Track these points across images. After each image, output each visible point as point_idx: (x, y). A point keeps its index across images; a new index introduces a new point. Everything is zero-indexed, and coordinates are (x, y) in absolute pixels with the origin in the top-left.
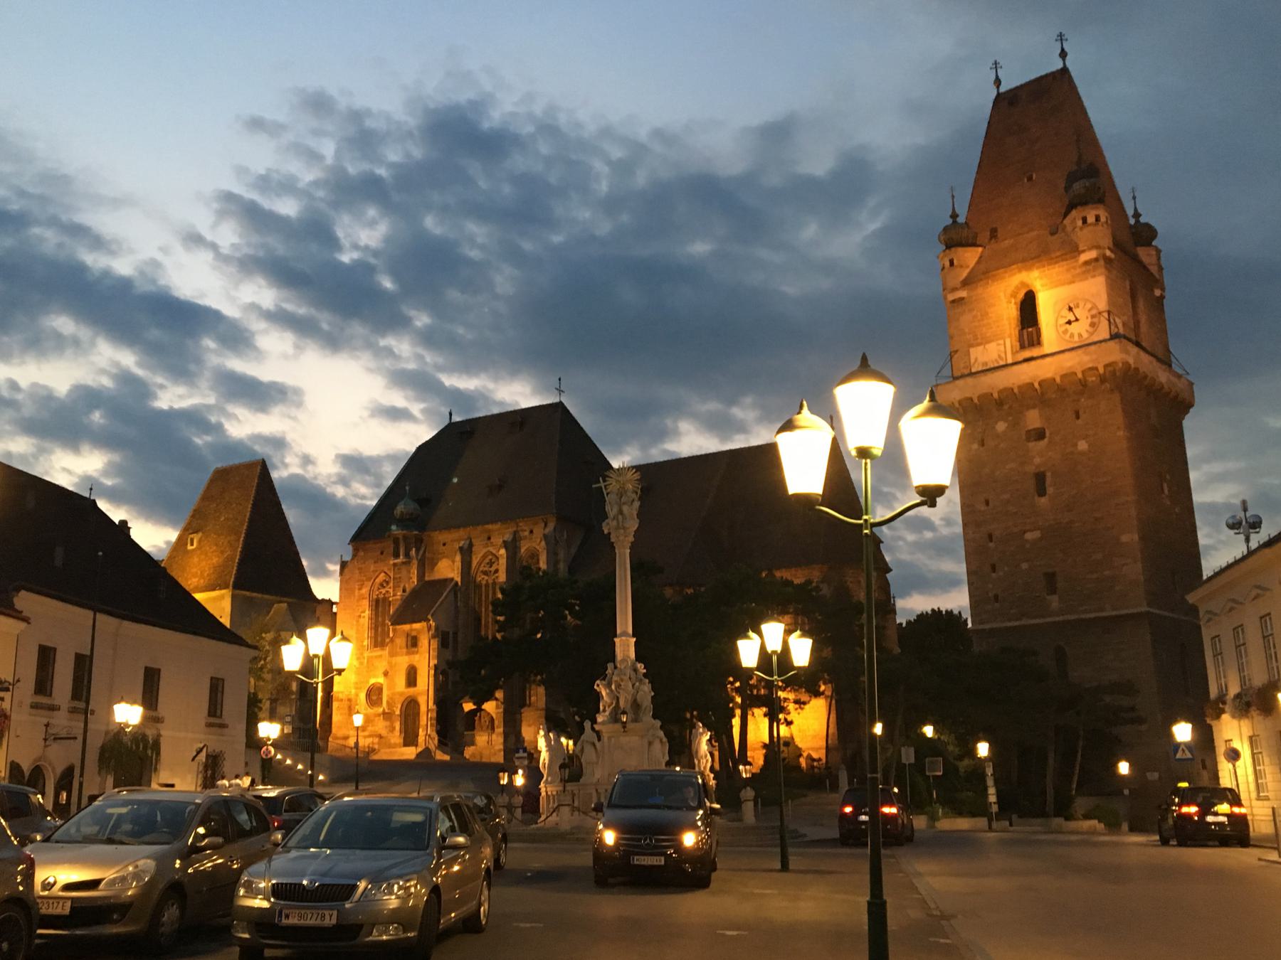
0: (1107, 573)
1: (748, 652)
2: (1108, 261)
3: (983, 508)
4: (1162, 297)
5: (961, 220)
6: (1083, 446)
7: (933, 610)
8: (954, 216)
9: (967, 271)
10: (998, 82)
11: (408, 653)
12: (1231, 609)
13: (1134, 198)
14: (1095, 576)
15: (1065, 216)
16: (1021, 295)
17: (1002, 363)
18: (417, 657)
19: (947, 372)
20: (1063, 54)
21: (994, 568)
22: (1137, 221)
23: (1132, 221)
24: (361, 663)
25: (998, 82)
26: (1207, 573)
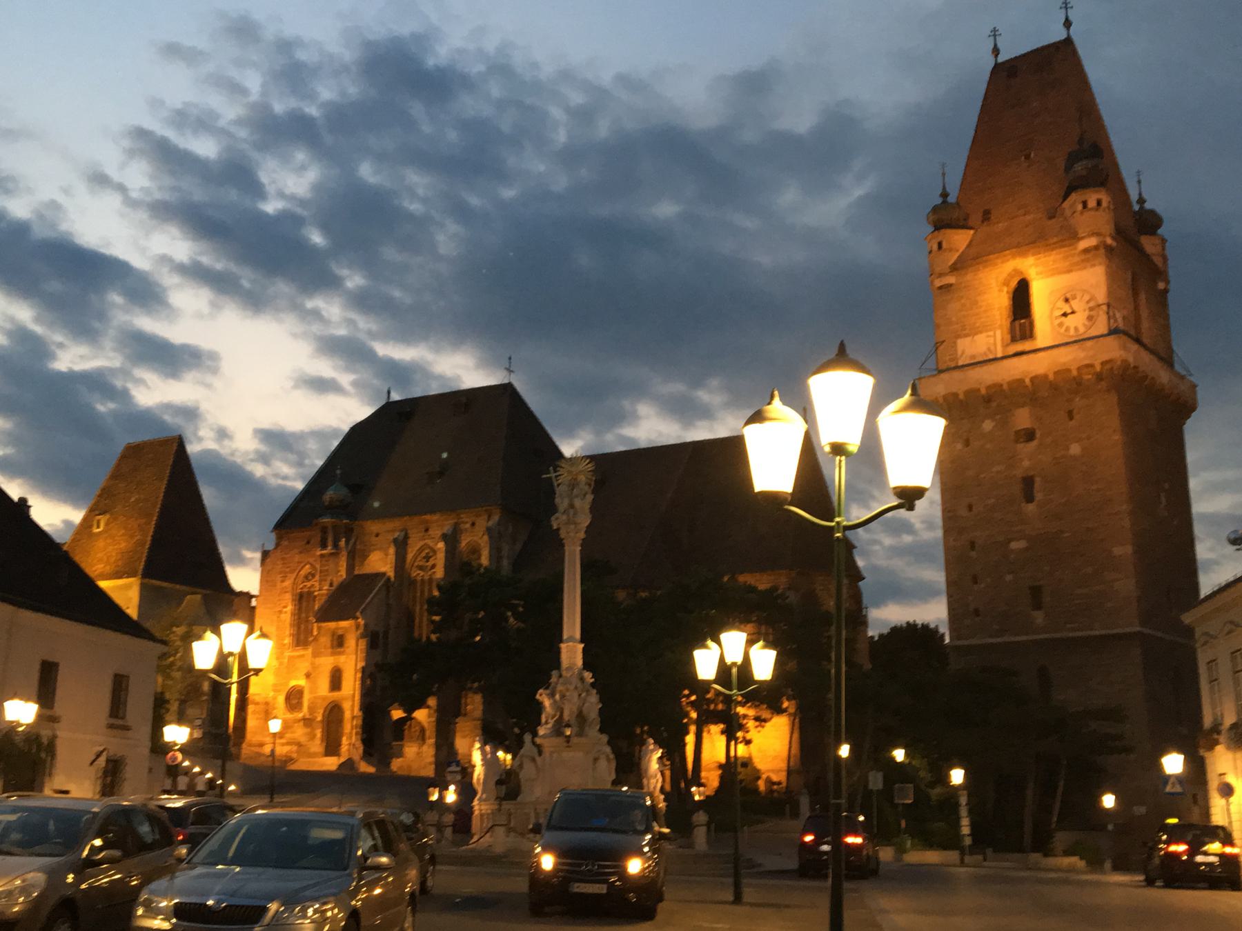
1: (705, 663)
2: (1109, 250)
4: (1166, 291)
5: (952, 199)
6: (1075, 449)
7: (908, 623)
8: (945, 195)
9: (957, 254)
10: (996, 51)
11: (333, 654)
12: (1230, 632)
13: (1139, 182)
15: (1064, 200)
16: (1014, 284)
17: (991, 357)
18: (342, 658)
19: (931, 364)
20: (1068, 24)
21: (975, 580)
22: (1142, 208)
23: (1136, 207)
24: (281, 664)
25: (996, 51)
26: (1204, 591)
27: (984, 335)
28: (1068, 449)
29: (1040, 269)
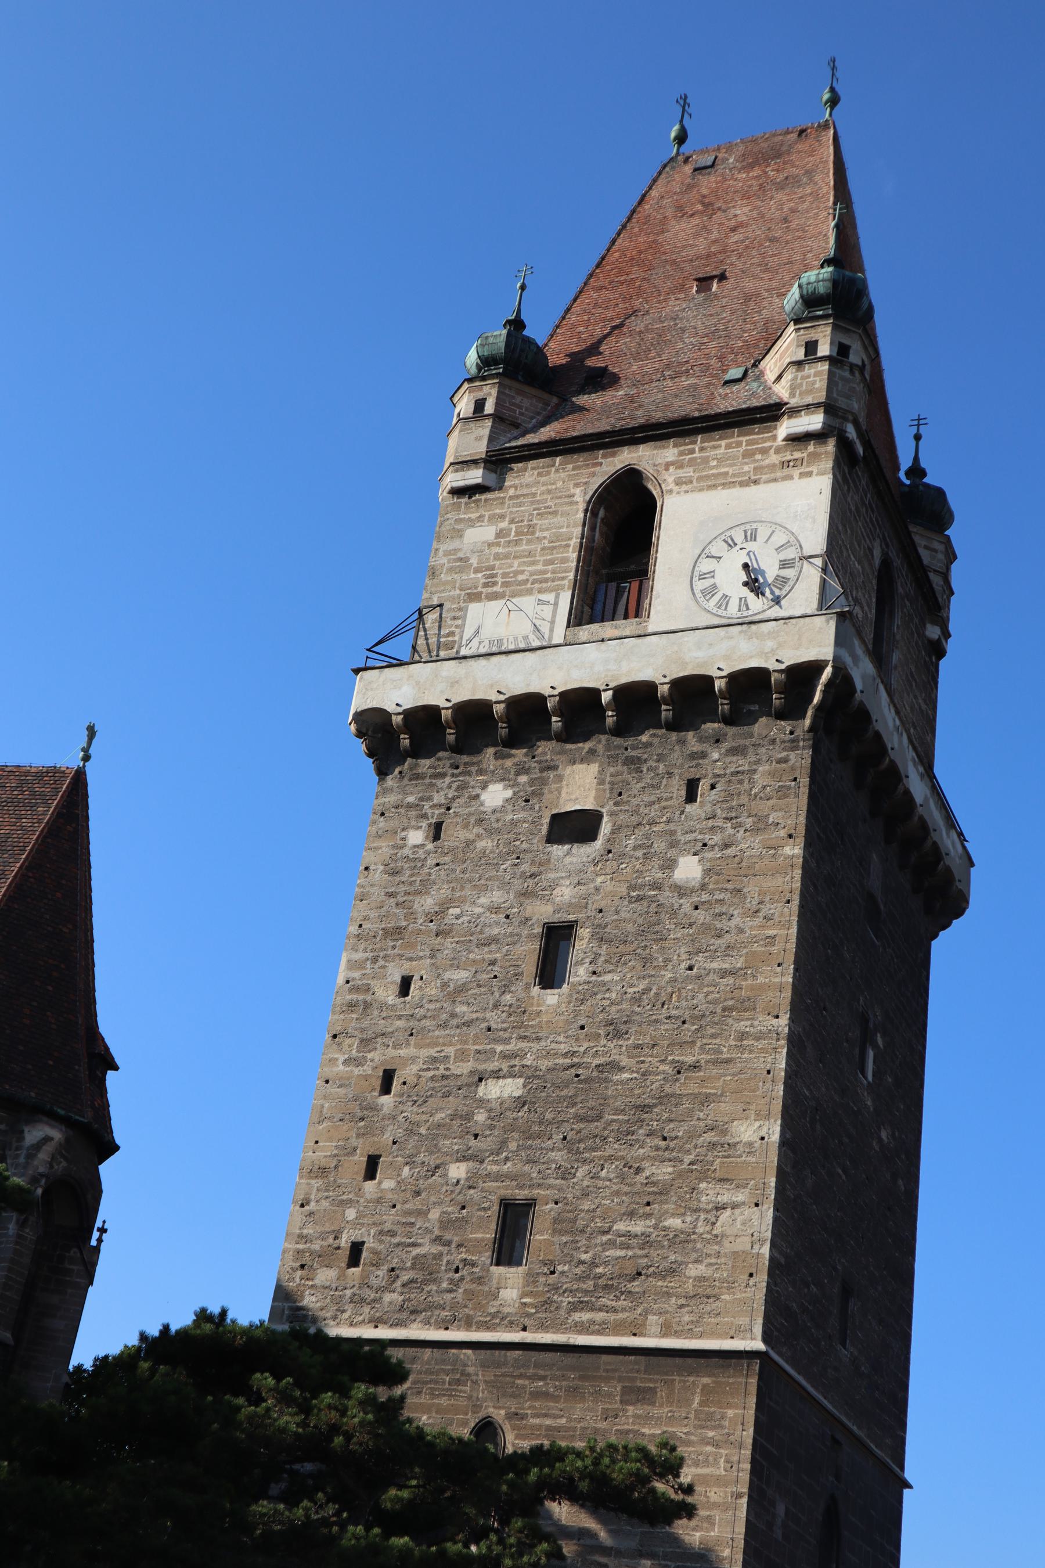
0: (675, 1222)
2: (844, 447)
4: (938, 651)
13: (918, 437)
14: (638, 1227)
28: (670, 865)
29: (688, 472)
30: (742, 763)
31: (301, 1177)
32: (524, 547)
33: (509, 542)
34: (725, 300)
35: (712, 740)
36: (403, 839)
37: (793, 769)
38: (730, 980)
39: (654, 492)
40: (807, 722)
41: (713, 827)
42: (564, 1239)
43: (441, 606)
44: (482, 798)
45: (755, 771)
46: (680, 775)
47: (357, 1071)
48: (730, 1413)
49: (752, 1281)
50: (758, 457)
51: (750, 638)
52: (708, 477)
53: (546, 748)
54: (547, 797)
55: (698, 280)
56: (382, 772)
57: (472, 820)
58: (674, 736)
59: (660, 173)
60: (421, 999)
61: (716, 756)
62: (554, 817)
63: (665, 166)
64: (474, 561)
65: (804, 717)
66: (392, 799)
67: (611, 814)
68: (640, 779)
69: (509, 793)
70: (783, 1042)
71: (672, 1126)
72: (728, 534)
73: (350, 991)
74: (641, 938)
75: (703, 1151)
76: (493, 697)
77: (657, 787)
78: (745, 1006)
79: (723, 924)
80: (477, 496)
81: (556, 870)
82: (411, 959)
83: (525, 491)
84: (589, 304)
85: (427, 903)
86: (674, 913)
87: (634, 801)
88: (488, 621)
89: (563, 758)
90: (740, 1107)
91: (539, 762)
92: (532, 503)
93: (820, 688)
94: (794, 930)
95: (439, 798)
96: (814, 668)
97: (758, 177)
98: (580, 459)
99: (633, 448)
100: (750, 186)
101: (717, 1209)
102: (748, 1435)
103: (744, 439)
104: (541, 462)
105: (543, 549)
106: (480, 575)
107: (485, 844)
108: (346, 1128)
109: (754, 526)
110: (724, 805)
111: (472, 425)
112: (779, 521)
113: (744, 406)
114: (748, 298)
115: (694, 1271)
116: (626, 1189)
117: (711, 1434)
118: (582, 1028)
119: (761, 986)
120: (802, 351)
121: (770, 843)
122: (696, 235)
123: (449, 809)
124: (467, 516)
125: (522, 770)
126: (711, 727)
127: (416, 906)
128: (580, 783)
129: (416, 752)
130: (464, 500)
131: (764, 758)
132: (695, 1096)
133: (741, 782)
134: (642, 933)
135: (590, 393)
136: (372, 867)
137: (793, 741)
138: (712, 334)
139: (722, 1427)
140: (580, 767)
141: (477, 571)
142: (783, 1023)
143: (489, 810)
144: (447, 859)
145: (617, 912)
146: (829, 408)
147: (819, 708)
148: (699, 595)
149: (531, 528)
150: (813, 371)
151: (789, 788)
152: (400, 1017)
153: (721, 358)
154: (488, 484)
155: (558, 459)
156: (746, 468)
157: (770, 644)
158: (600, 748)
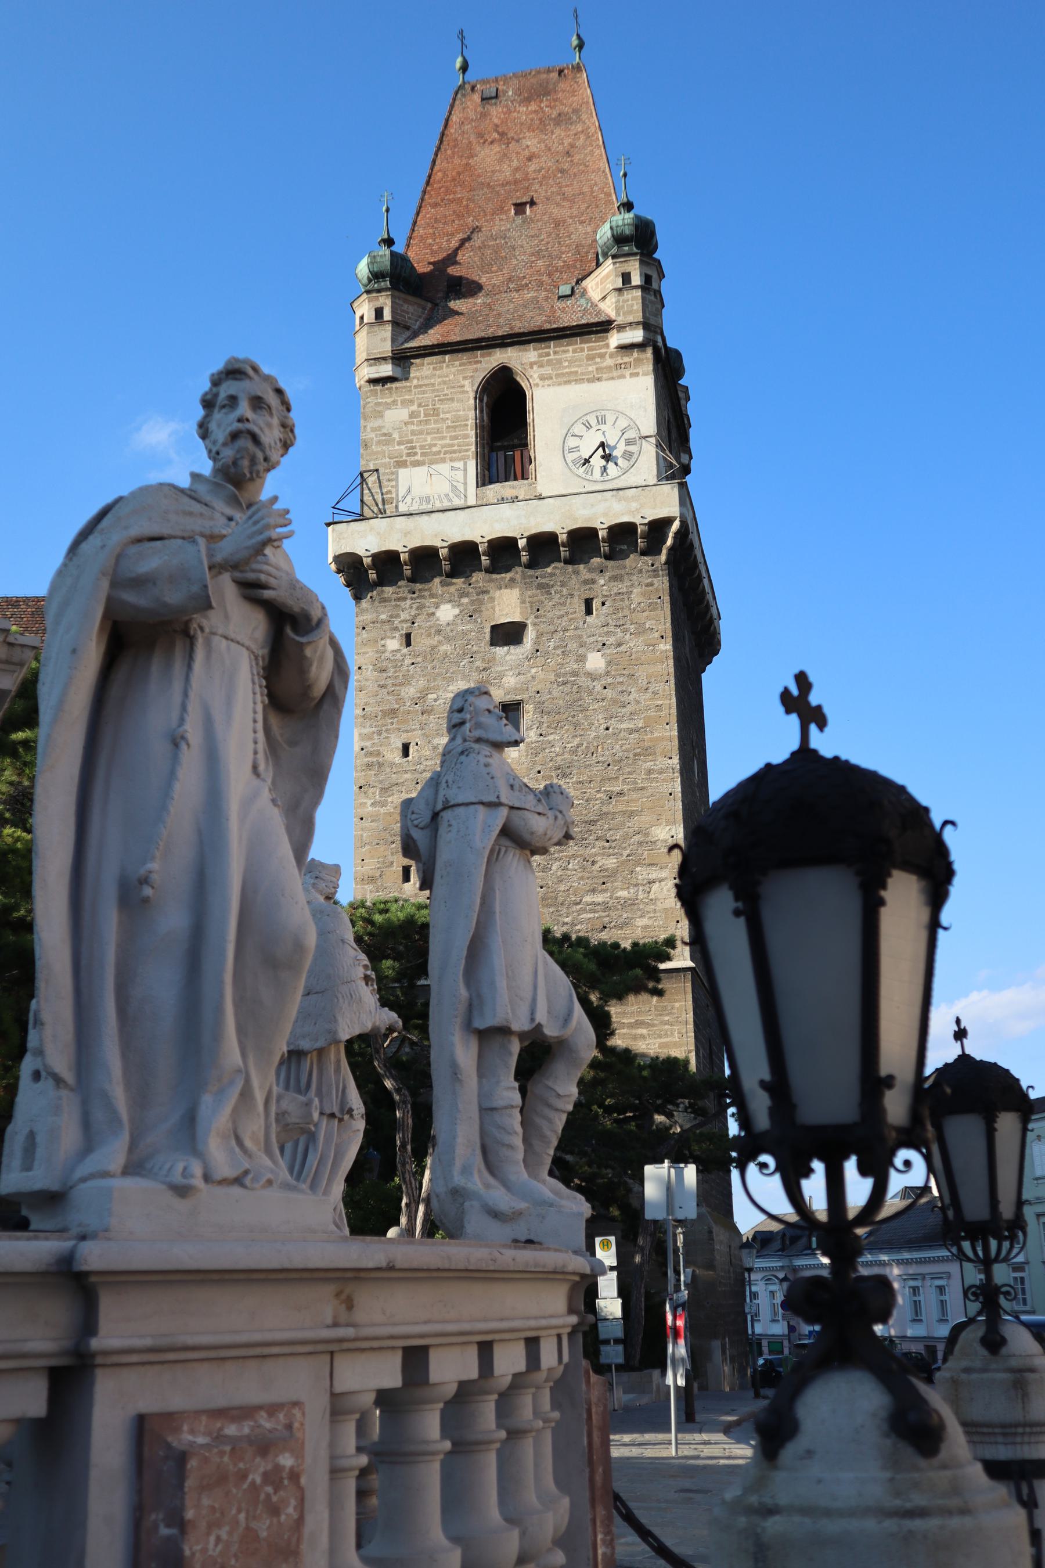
0: (623, 894)
3: (397, 757)
6: (595, 662)
14: (599, 898)
27: (444, 468)
28: (582, 659)
29: (547, 370)
30: (622, 587)
31: (357, 884)
32: (433, 426)
33: (421, 421)
34: (540, 224)
35: (598, 571)
36: (383, 646)
37: (657, 590)
38: (635, 735)
39: (523, 384)
40: (663, 557)
41: (608, 632)
42: (551, 910)
43: (377, 470)
44: (437, 614)
45: (631, 592)
46: (579, 596)
47: (382, 810)
48: (677, 1005)
49: (679, 925)
50: (598, 360)
51: (620, 501)
52: (563, 374)
53: (478, 577)
54: (485, 613)
55: (515, 205)
56: (358, 598)
57: (433, 631)
58: (570, 568)
59: (454, 99)
60: (420, 758)
61: (602, 582)
62: (493, 627)
63: (457, 93)
64: (396, 436)
65: (659, 553)
66: (368, 617)
67: (534, 625)
68: (551, 599)
69: (457, 611)
70: (677, 774)
71: (611, 832)
72: (585, 418)
73: (366, 755)
74: (570, 710)
75: (635, 847)
76: (438, 544)
77: (564, 604)
78: (648, 752)
79: (625, 698)
80: (389, 385)
81: (501, 665)
82: (406, 731)
83: (426, 382)
84: (430, 218)
85: (410, 692)
86: (590, 692)
87: (549, 615)
88: (416, 484)
89: (492, 584)
90: (655, 818)
91: (475, 588)
92: (433, 391)
93: (671, 535)
94: (674, 700)
95: (404, 616)
96: (667, 522)
97: (536, 112)
98: (465, 357)
99: (503, 350)
100: (532, 120)
101: (650, 883)
102: (690, 1016)
103: (586, 346)
104: (434, 358)
105: (448, 427)
106: (403, 447)
107: (446, 648)
108: (382, 849)
109: (603, 413)
110: (614, 616)
111: (376, 328)
112: (619, 409)
113: (583, 322)
114: (558, 224)
115: (640, 922)
116: (587, 875)
117: (667, 1018)
118: (539, 772)
119: (657, 739)
120: (620, 280)
121: (648, 642)
122: (500, 161)
123: (413, 623)
124: (384, 401)
125: (463, 594)
126: (596, 561)
127: (402, 694)
128: (507, 602)
129: (381, 582)
130: (379, 388)
131: (636, 583)
132: (624, 812)
133: (622, 600)
134: (570, 706)
135: (455, 299)
136: (364, 667)
137: (654, 571)
138: (537, 254)
139: (673, 1014)
140: (506, 592)
141: (399, 443)
142: (676, 760)
143: (444, 623)
144: (419, 659)
145: (550, 693)
146: (646, 326)
147: (671, 549)
148: (571, 464)
149: (436, 412)
150: (630, 296)
151: (657, 603)
152: (407, 772)
153: (550, 275)
154: (396, 375)
155: (447, 357)
156: (590, 369)
157: (634, 505)
158: (518, 577)
